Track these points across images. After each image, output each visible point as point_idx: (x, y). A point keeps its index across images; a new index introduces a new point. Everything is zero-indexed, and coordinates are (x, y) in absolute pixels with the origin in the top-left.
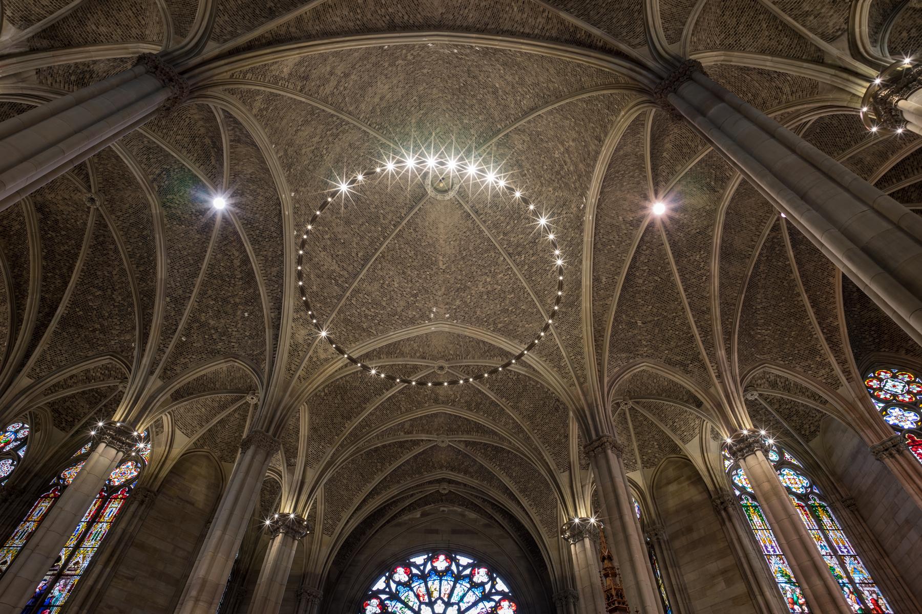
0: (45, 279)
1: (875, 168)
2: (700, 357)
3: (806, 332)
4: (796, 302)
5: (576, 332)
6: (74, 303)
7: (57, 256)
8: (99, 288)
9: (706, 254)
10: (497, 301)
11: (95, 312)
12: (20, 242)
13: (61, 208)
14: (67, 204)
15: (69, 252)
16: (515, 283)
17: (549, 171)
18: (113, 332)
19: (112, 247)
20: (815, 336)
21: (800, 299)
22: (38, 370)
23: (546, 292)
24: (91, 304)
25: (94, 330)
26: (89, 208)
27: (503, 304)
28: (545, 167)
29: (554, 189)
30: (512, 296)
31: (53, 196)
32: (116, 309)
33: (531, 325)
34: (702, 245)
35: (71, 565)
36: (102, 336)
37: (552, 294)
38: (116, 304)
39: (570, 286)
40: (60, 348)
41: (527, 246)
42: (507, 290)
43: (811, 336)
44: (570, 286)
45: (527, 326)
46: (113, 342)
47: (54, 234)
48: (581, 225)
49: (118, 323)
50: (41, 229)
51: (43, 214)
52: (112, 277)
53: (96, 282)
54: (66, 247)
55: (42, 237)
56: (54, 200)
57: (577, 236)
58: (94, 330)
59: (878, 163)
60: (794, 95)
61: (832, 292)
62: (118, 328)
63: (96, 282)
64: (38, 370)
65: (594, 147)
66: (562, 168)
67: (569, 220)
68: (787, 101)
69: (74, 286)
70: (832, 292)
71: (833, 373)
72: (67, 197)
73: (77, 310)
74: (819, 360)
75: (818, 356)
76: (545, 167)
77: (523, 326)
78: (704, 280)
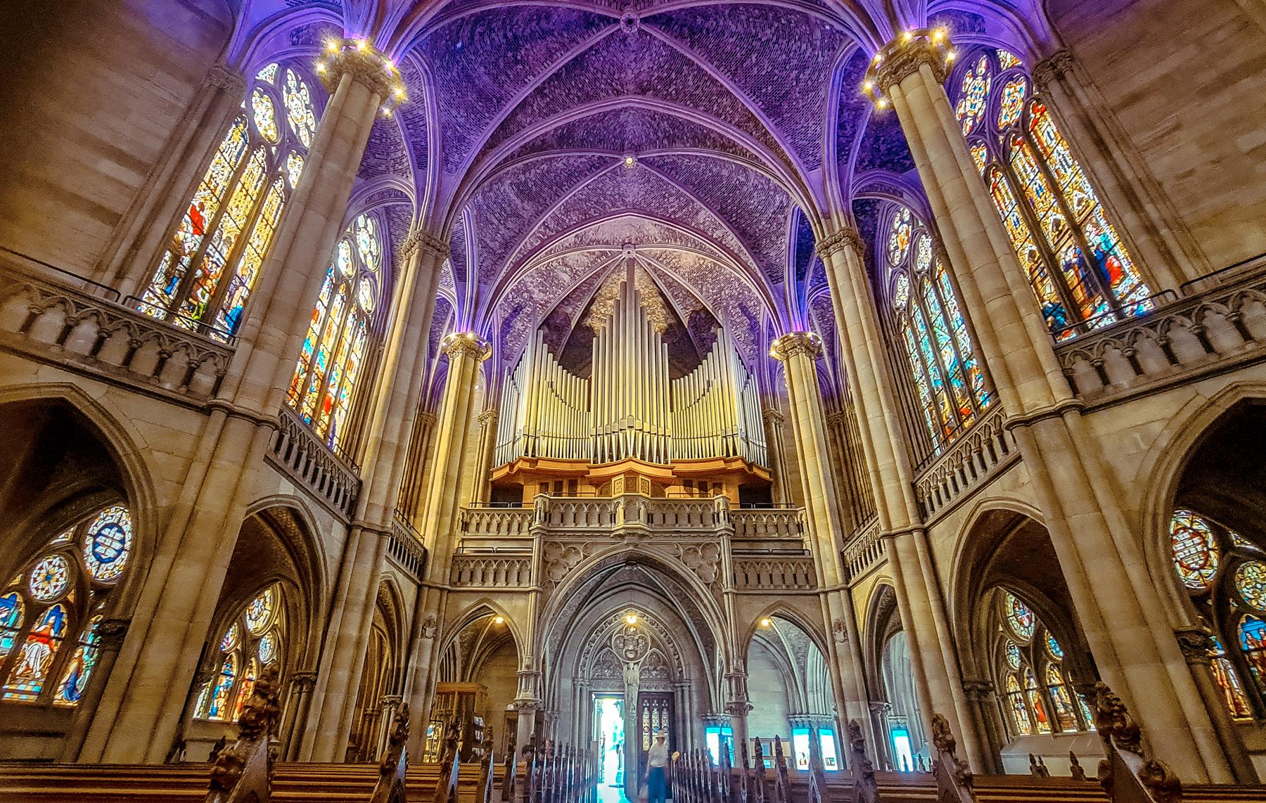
0: (718, 115)
6: (755, 91)
7: (698, 92)
8: (748, 55)
11: (776, 71)
12: (681, 127)
13: (645, 67)
14: (643, 59)
15: (695, 76)
18: (808, 54)
19: (699, 20)
22: (811, 158)
24: (764, 73)
25: (797, 79)
26: (640, 31)
31: (630, 71)
32: (780, 41)
35: (1075, 209)
36: (808, 72)
38: (774, 39)
40: (799, 126)
46: (820, 59)
47: (674, 87)
49: (799, 43)
50: (664, 98)
51: (649, 90)
52: (739, 34)
53: (739, 55)
54: (690, 78)
55: (674, 100)
56: (636, 72)
58: (797, 79)
62: (804, 46)
63: (739, 55)
64: (811, 158)
69: (732, 84)
72: (633, 56)
73: (764, 90)
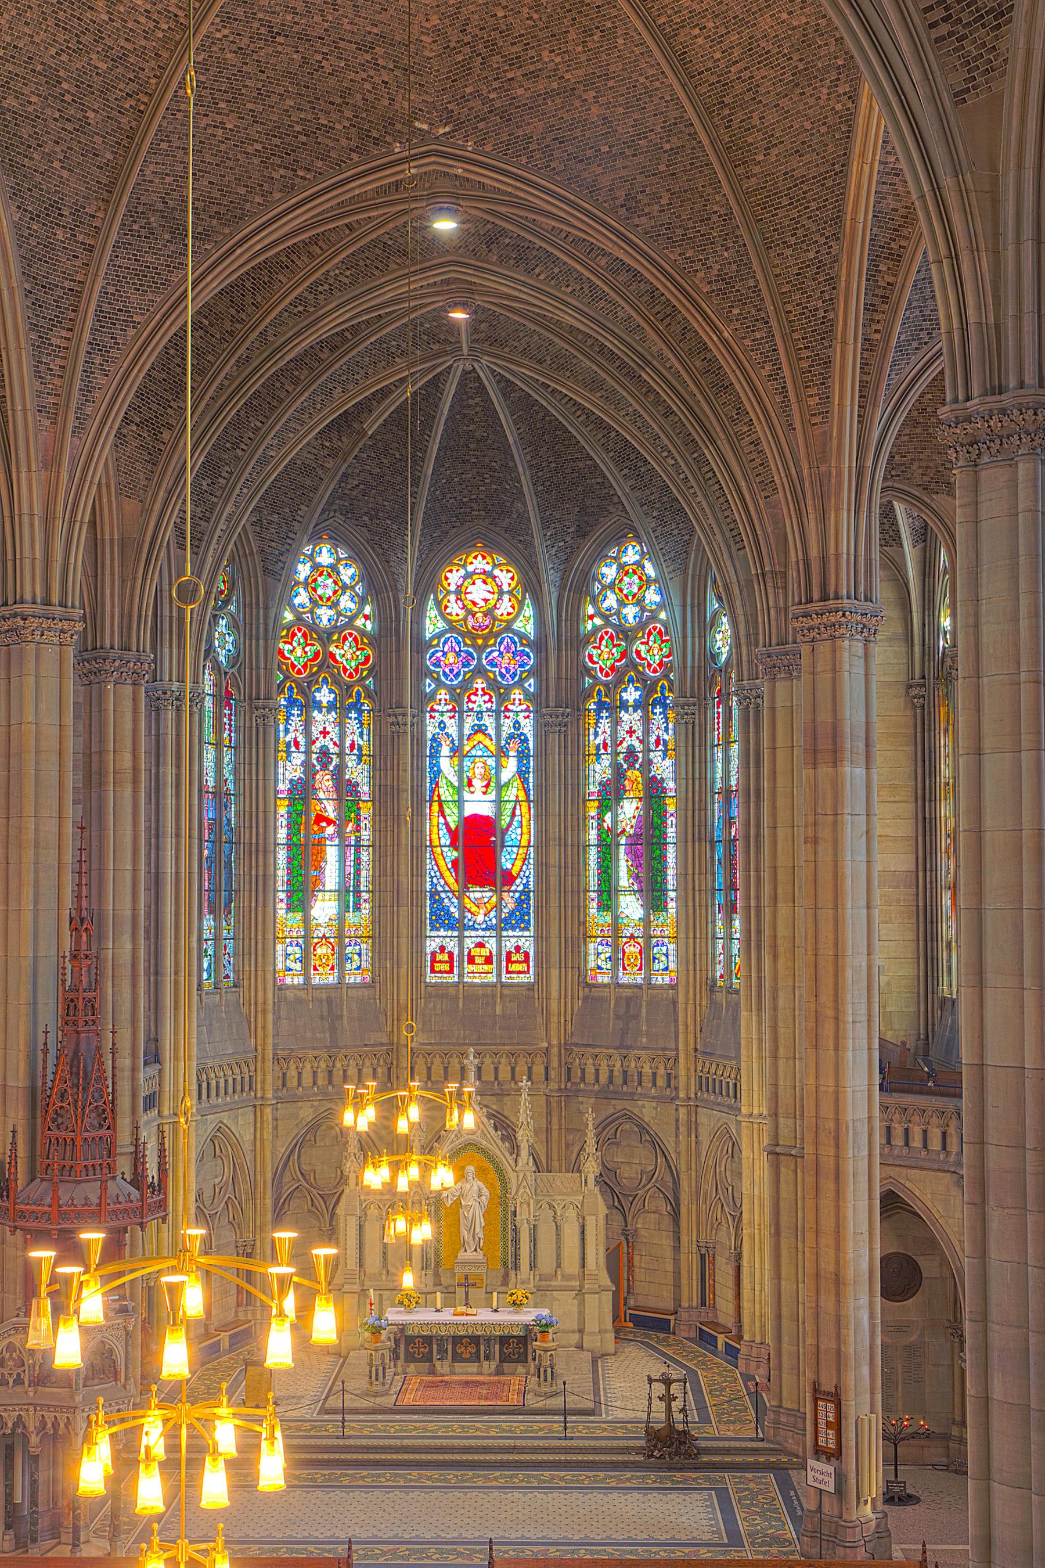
1: (568, 374)
2: (166, 435)
3: (236, 434)
4: (278, 385)
5: (134, 297)
9: (346, 281)
10: (61, 37)
16: (143, 52)
17: (492, 21)
20: (239, 452)
21: (290, 389)
23: (164, 146)
27: (64, 57)
28: (500, 14)
29: (436, 30)
30: (103, 66)
33: (65, 174)
34: (362, 263)
37: (168, 160)
39: (217, 194)
41: (256, 24)
42: (109, 42)
43: (236, 446)
44: (217, 194)
45: (56, 164)
48: (376, 142)
57: (344, 142)
59: (580, 378)
60: (752, 448)
61: (319, 406)
65: (605, 181)
66: (515, 62)
67: (370, 97)
68: (739, 436)
70: (319, 406)
71: (202, 523)
74: (205, 487)
75: (209, 481)
76: (500, 14)
77: (49, 157)
78: (296, 311)
